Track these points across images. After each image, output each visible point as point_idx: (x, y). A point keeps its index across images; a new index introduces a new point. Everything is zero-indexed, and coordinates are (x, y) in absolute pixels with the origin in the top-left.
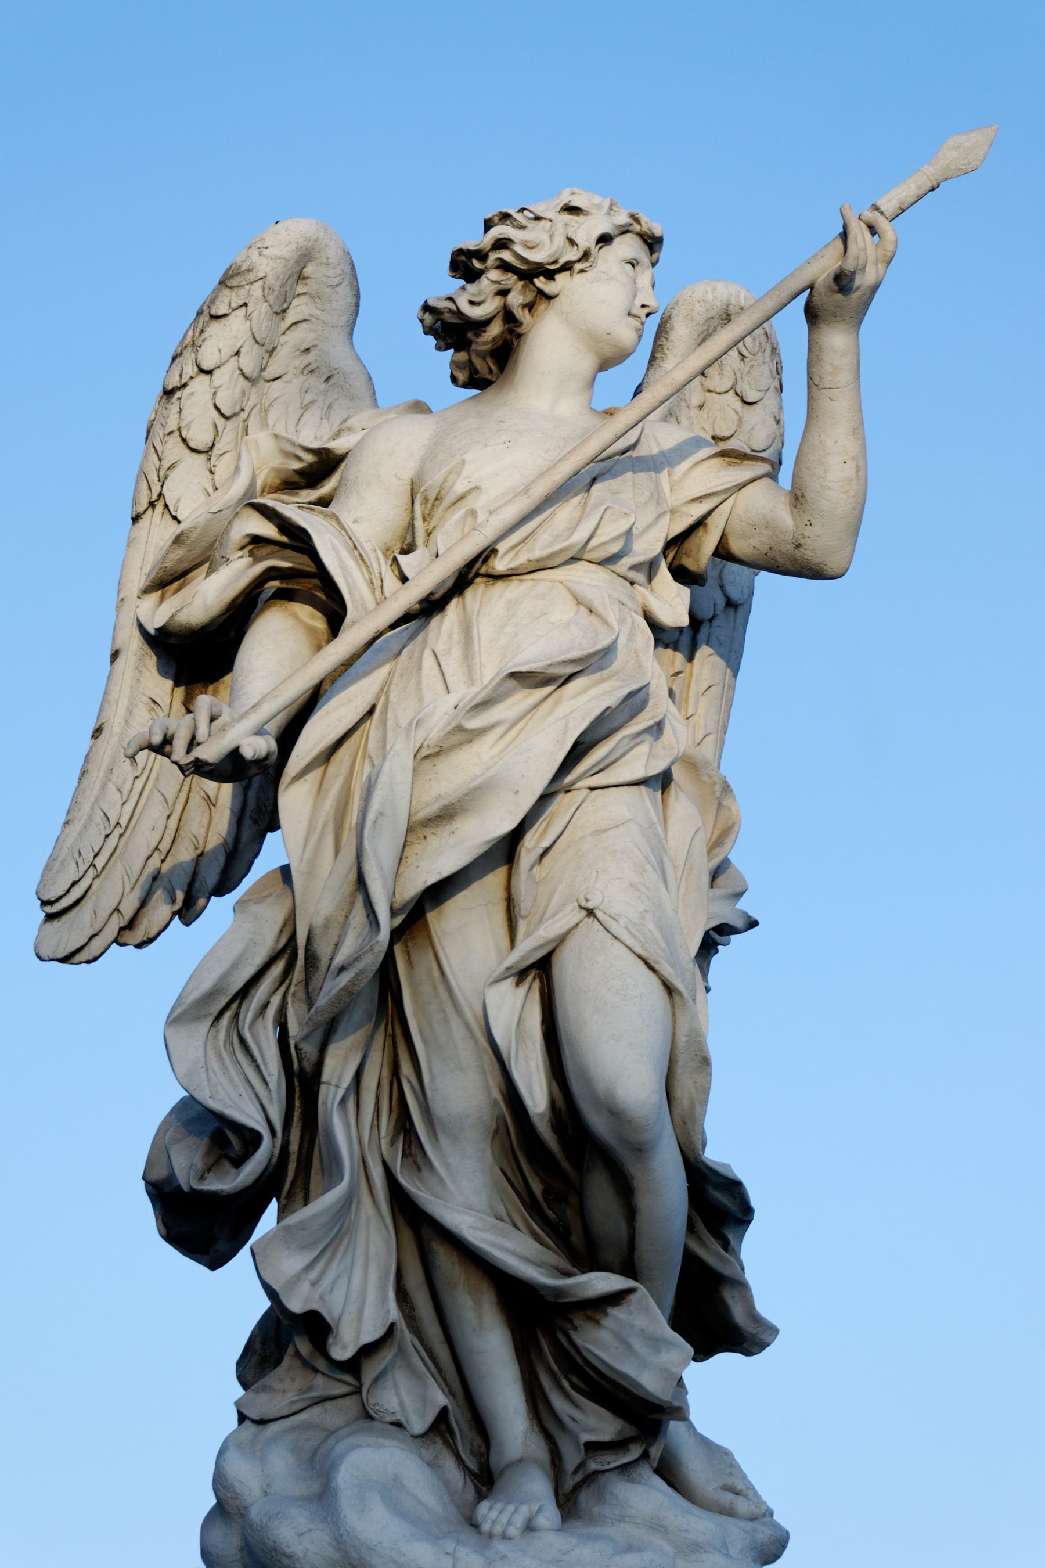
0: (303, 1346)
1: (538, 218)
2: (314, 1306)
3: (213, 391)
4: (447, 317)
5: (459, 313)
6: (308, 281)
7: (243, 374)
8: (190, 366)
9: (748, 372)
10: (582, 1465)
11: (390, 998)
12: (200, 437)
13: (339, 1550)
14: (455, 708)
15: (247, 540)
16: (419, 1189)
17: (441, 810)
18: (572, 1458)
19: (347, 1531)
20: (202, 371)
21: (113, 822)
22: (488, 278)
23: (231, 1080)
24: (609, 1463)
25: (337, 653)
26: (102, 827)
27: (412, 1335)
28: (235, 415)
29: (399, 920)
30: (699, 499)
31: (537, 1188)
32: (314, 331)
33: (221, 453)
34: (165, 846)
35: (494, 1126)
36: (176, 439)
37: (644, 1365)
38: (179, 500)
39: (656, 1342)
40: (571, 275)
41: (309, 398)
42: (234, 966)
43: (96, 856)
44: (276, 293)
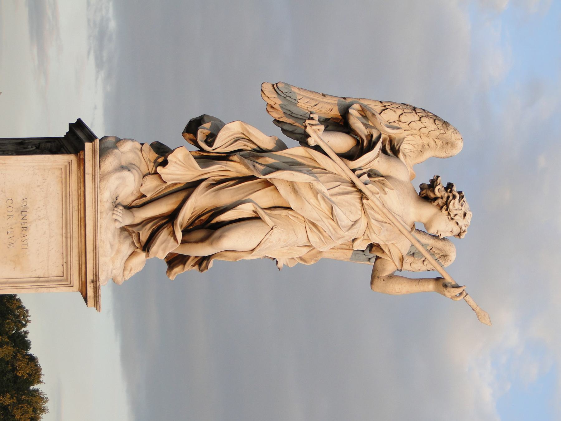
0: (161, 160)
1: (462, 206)
4: (435, 183)
5: (436, 186)
6: (446, 145)
7: (420, 129)
8: (422, 115)
10: (134, 232)
13: (107, 173)
15: (372, 134)
16: (201, 188)
17: (296, 190)
18: (135, 229)
20: (420, 118)
23: (226, 138)
24: (135, 239)
27: (165, 187)
29: (269, 180)
30: (389, 251)
34: (293, 115)
36: (402, 112)
37: (159, 247)
38: (386, 113)
39: (164, 250)
40: (447, 215)
41: (416, 146)
42: (256, 137)
44: (442, 137)
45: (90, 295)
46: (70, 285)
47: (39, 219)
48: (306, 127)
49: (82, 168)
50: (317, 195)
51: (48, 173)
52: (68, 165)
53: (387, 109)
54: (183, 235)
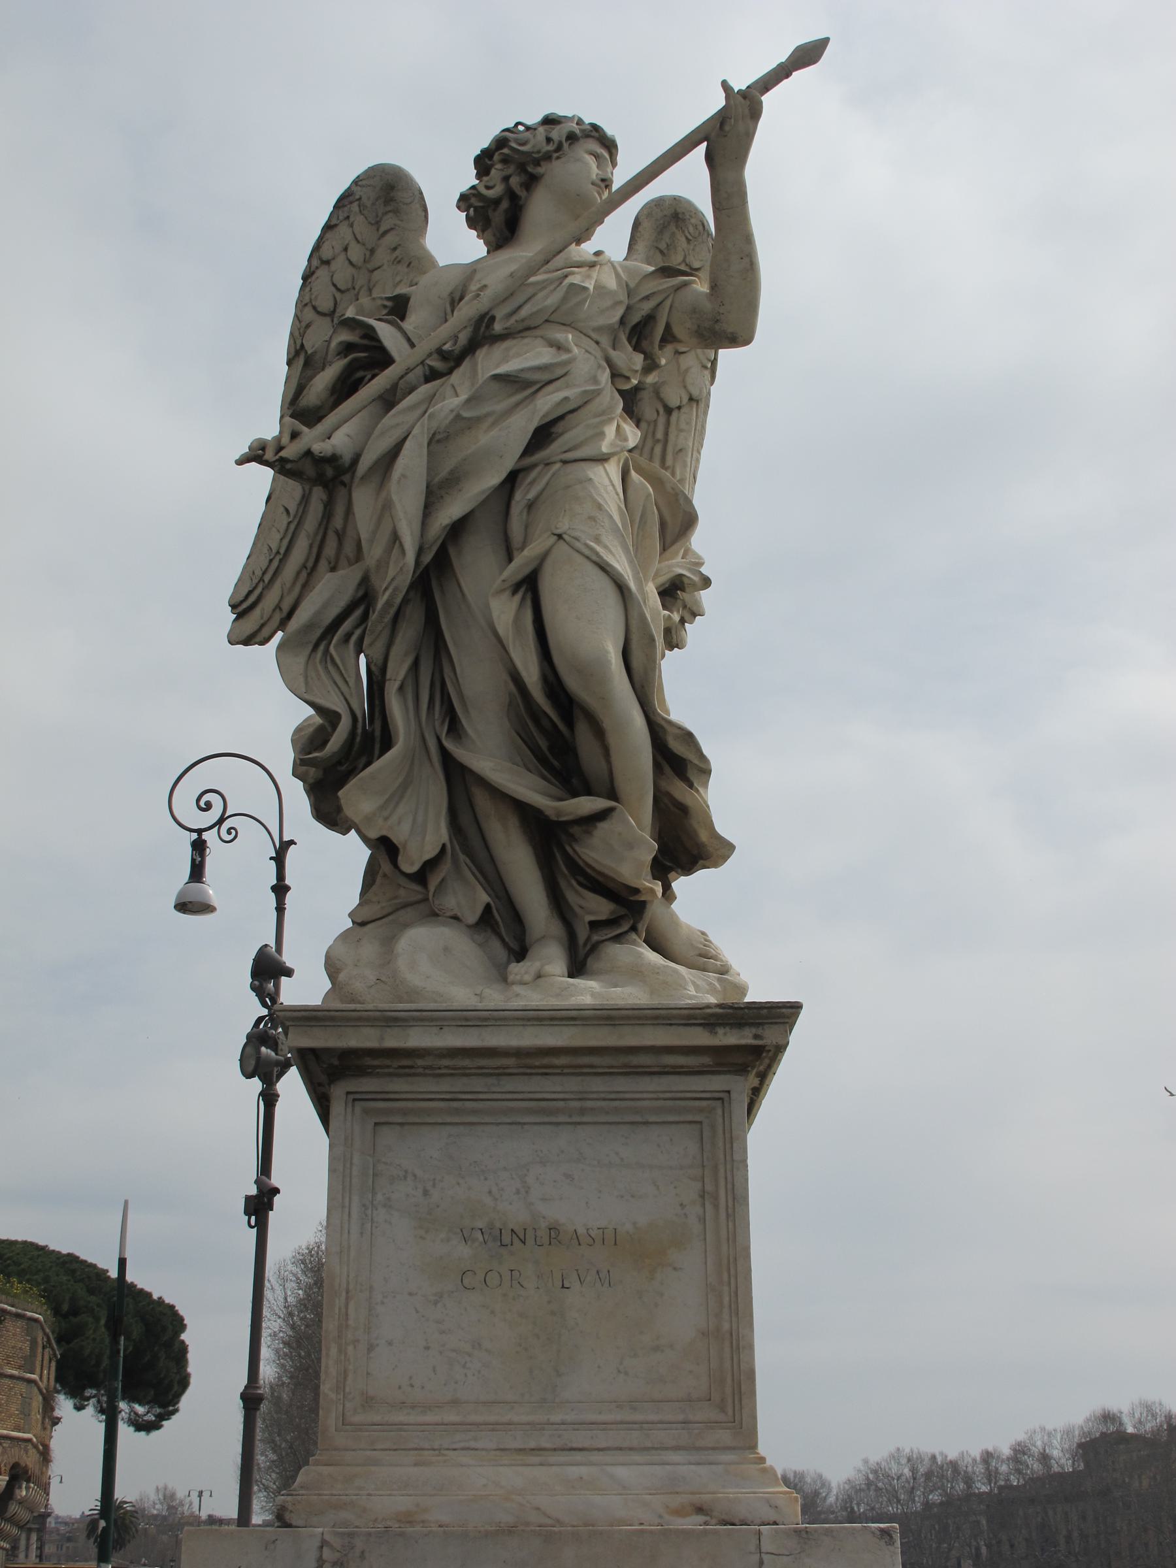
2: (384, 833)
3: (331, 274)
7: (351, 263)
9: (693, 250)
10: (588, 939)
11: (630, 819)
16: (457, 748)
18: (582, 933)
21: (274, 551)
22: (496, 169)
24: (606, 935)
26: (267, 555)
28: (348, 290)
31: (543, 744)
33: (340, 315)
34: (310, 564)
41: (398, 279)
45: (751, 1035)
46: (726, 1099)
47: (527, 1192)
49: (369, 1061)
50: (465, 418)
51: (386, 1163)
52: (362, 1103)
53: (302, 346)
54: (589, 792)
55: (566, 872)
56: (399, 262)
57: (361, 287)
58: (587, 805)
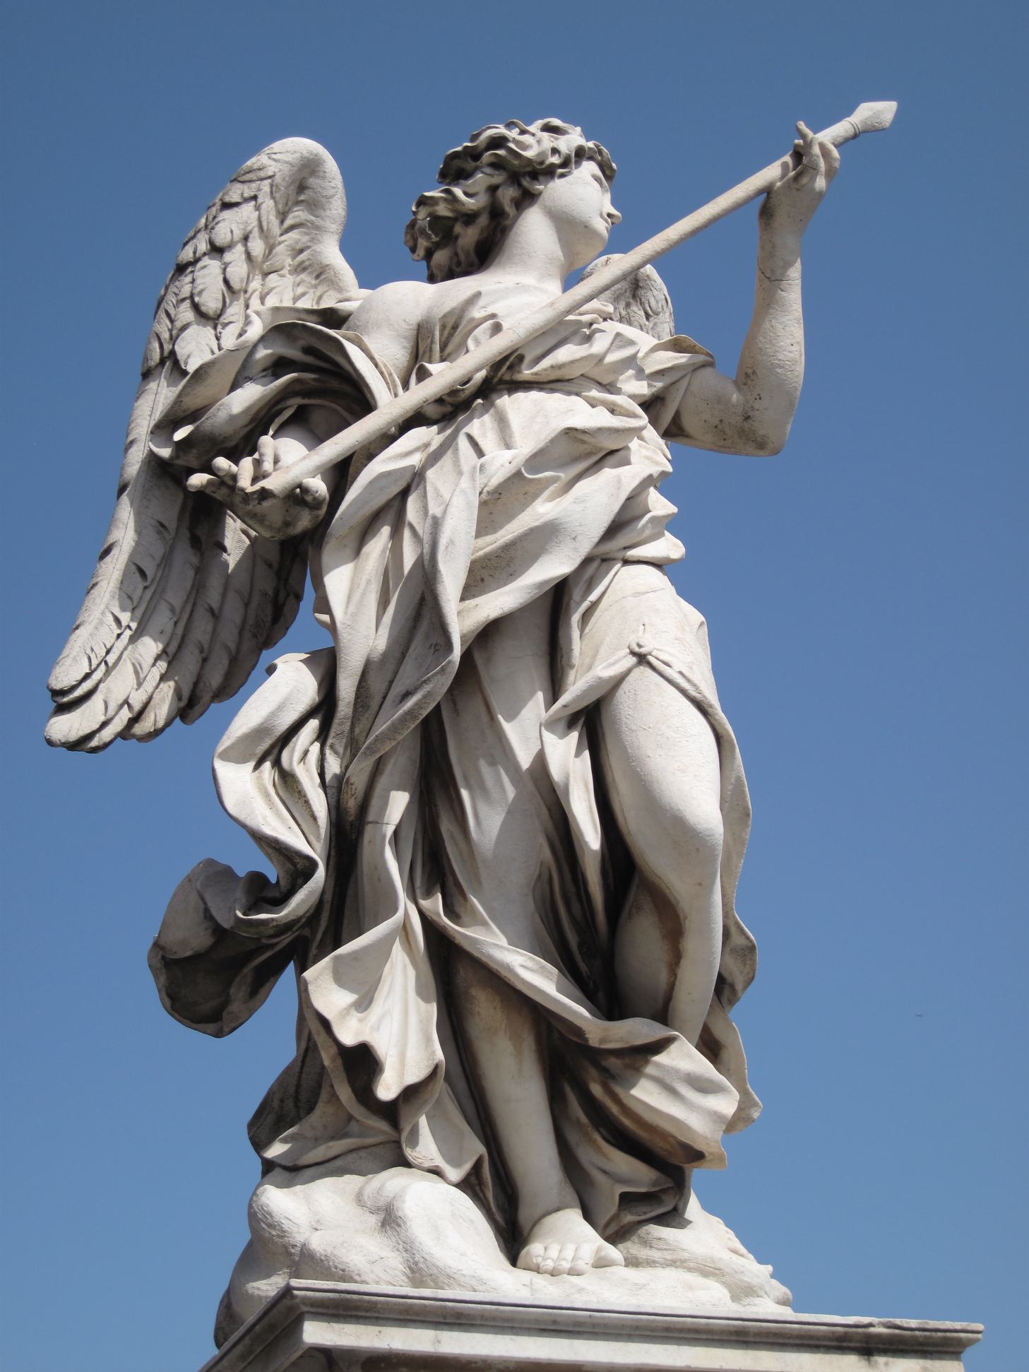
3: (223, 266)
9: (652, 328)
10: (616, 1217)
12: (210, 302)
14: (510, 463)
19: (423, 1258)
23: (279, 815)
24: (645, 1213)
25: (391, 413)
31: (573, 939)
32: (306, 234)
35: (537, 873)
38: (189, 356)
41: (300, 290)
43: (108, 652)
44: (281, 193)
48: (264, 494)
53: (173, 353)
55: (584, 1119)
56: (304, 269)
57: (254, 291)
58: (637, 1030)
